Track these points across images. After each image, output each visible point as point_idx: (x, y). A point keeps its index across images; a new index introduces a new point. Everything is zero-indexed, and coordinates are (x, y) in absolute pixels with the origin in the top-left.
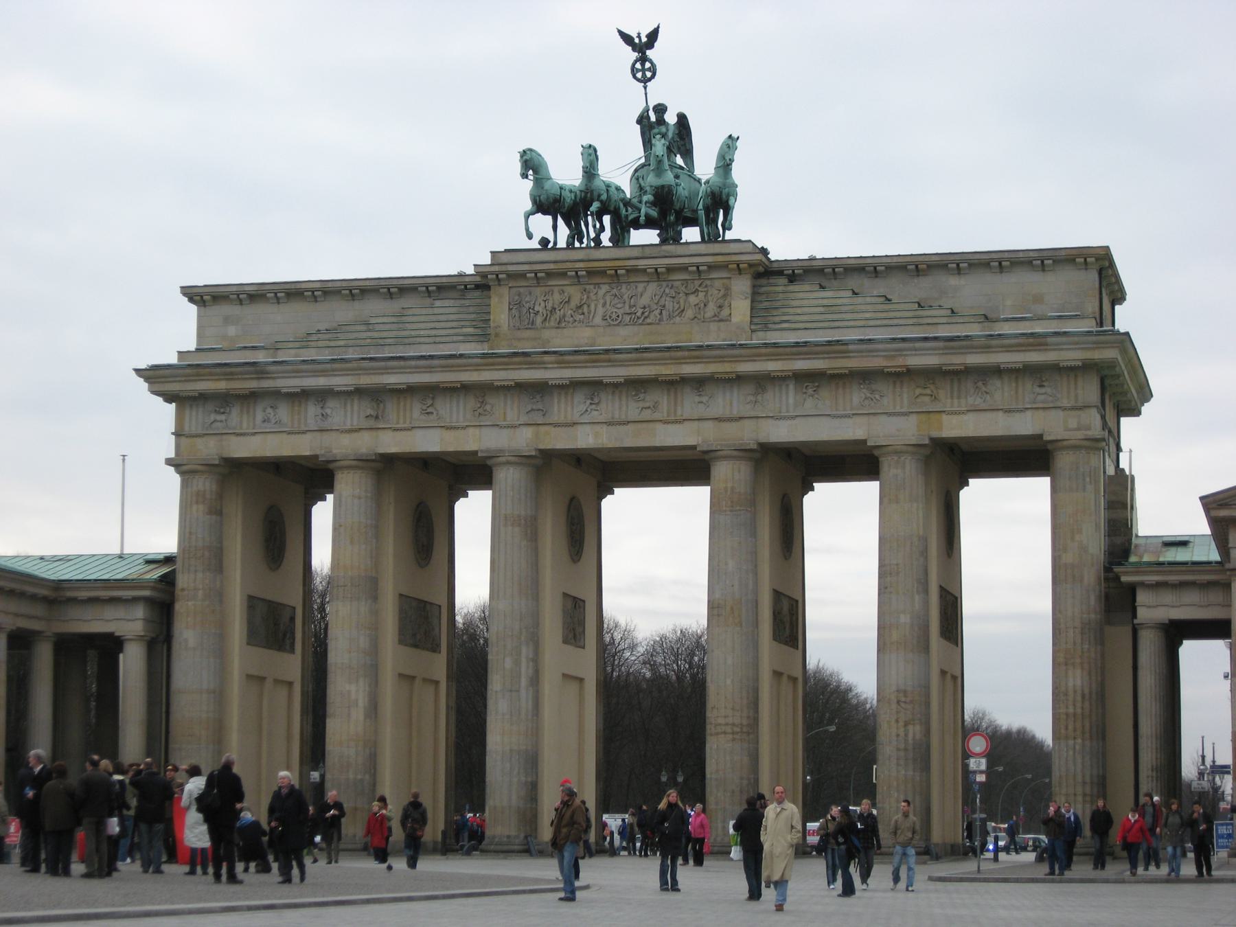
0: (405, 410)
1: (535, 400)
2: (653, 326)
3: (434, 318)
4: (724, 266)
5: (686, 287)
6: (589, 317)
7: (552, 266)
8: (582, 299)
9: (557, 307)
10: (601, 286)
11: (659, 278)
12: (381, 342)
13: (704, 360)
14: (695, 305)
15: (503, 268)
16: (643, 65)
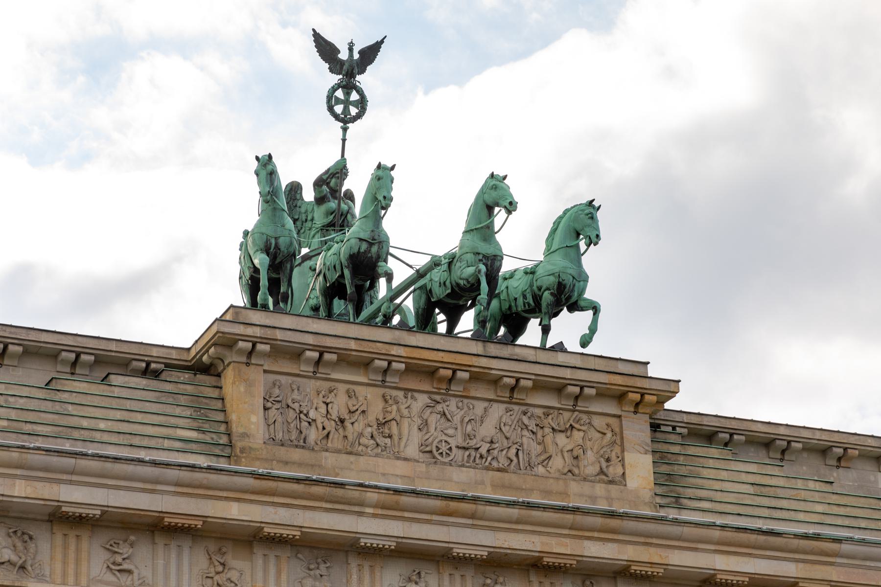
0: (78, 561)
1: (318, 572)
2: (506, 474)
3: (114, 403)
4: (620, 397)
5: (553, 418)
6: (399, 443)
7: (353, 345)
8: (385, 411)
9: (347, 417)
10: (416, 395)
11: (511, 397)
12: (28, 428)
13: (621, 537)
14: (567, 451)
15: (269, 333)
16: (348, 94)
